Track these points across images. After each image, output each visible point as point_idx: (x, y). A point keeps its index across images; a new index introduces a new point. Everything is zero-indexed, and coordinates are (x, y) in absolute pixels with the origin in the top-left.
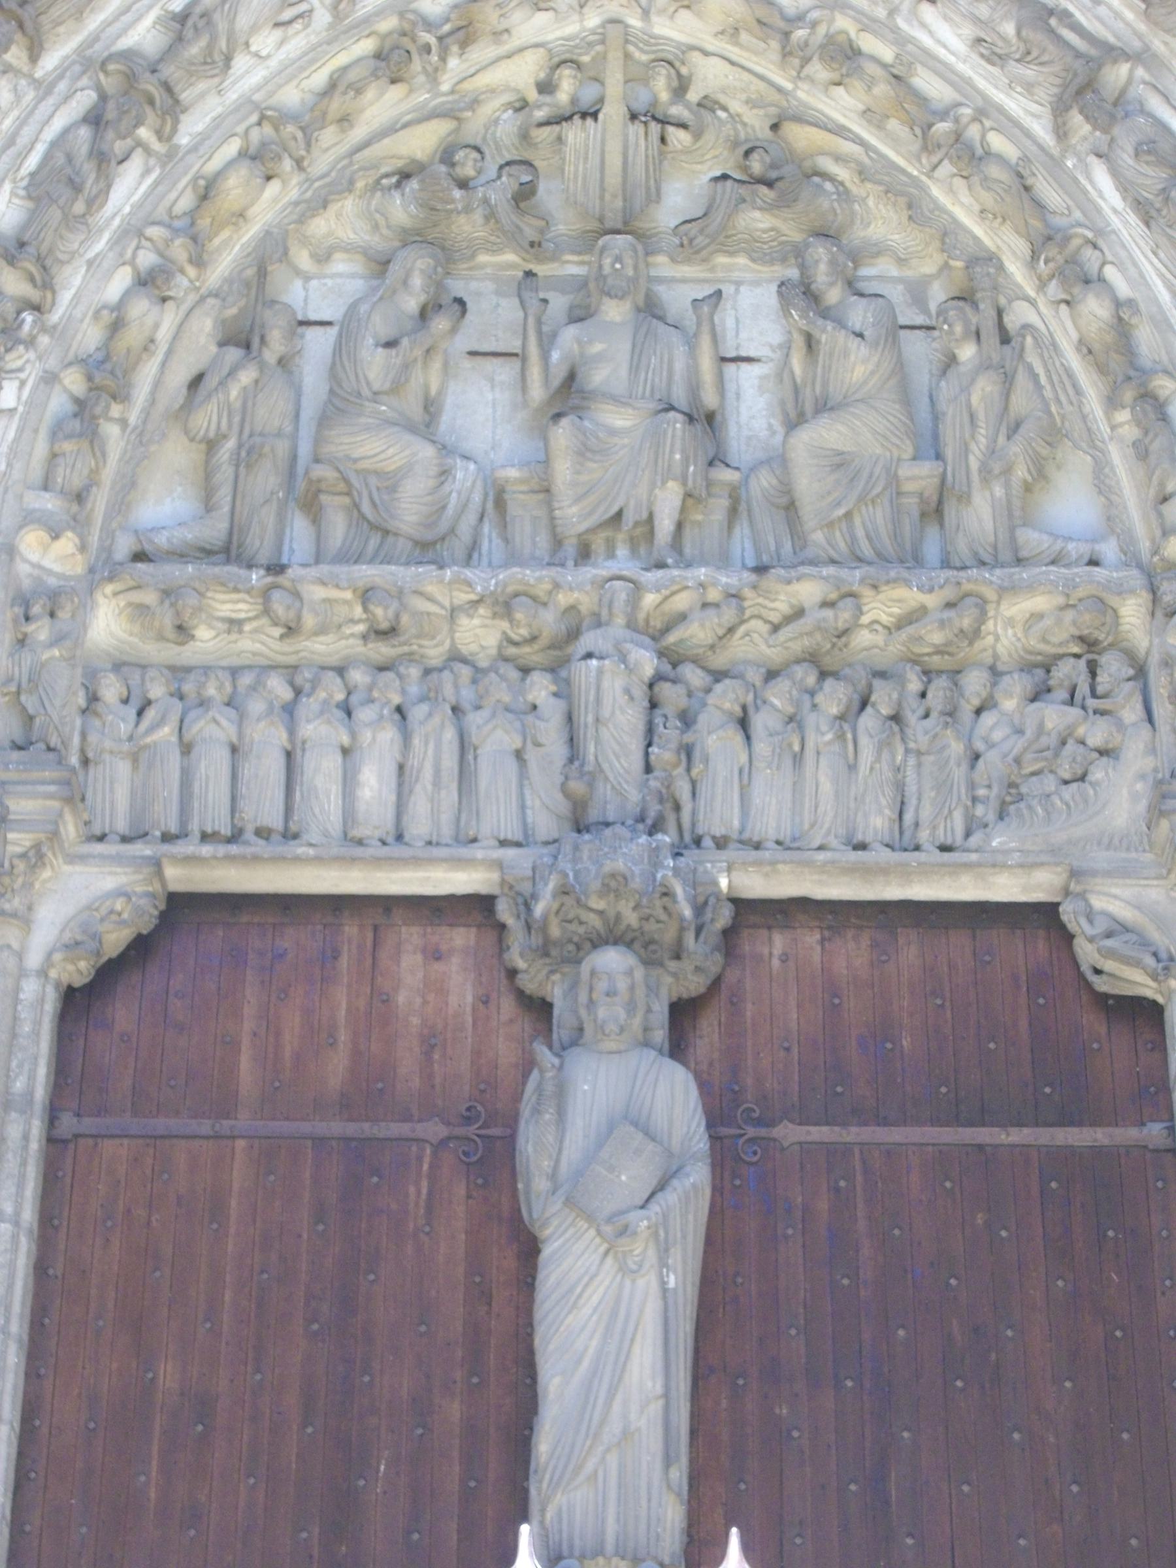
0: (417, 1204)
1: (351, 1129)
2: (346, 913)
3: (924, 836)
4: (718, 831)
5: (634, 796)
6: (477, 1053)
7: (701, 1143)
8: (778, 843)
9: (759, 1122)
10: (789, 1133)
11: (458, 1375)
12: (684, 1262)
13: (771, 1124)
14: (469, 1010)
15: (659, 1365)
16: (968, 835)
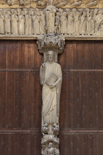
0: (28, 80)
1: (20, 70)
2: (18, 42)
3: (89, 33)
4: (64, 33)
5: (53, 29)
6: (35, 60)
7: (61, 75)
8: (71, 34)
9: (68, 69)
10: (72, 70)
11: (33, 100)
12: (59, 89)
13: (70, 69)
14: (33, 55)
15: (56, 101)
16: (94, 32)
